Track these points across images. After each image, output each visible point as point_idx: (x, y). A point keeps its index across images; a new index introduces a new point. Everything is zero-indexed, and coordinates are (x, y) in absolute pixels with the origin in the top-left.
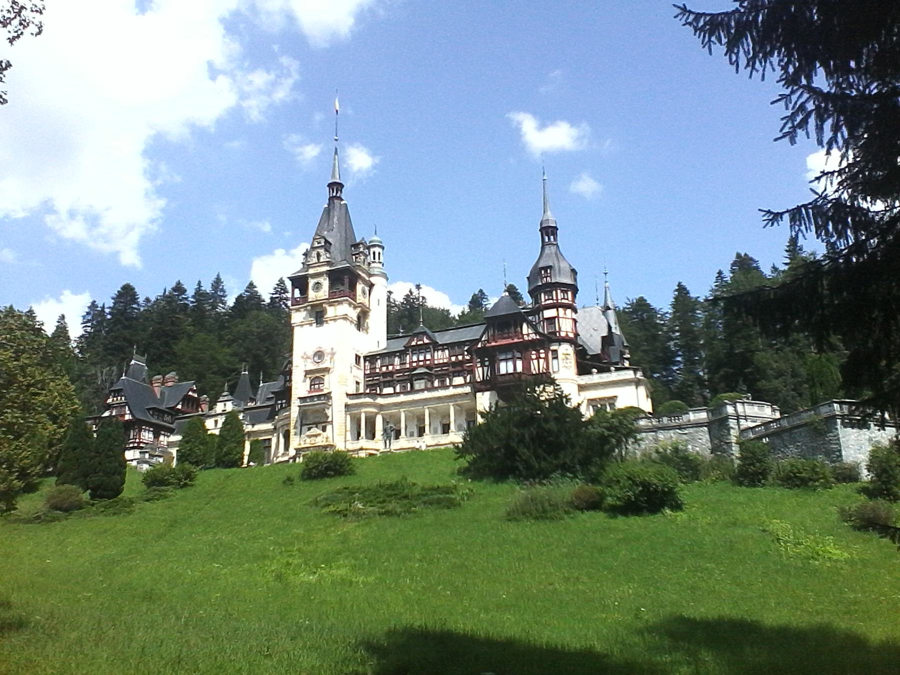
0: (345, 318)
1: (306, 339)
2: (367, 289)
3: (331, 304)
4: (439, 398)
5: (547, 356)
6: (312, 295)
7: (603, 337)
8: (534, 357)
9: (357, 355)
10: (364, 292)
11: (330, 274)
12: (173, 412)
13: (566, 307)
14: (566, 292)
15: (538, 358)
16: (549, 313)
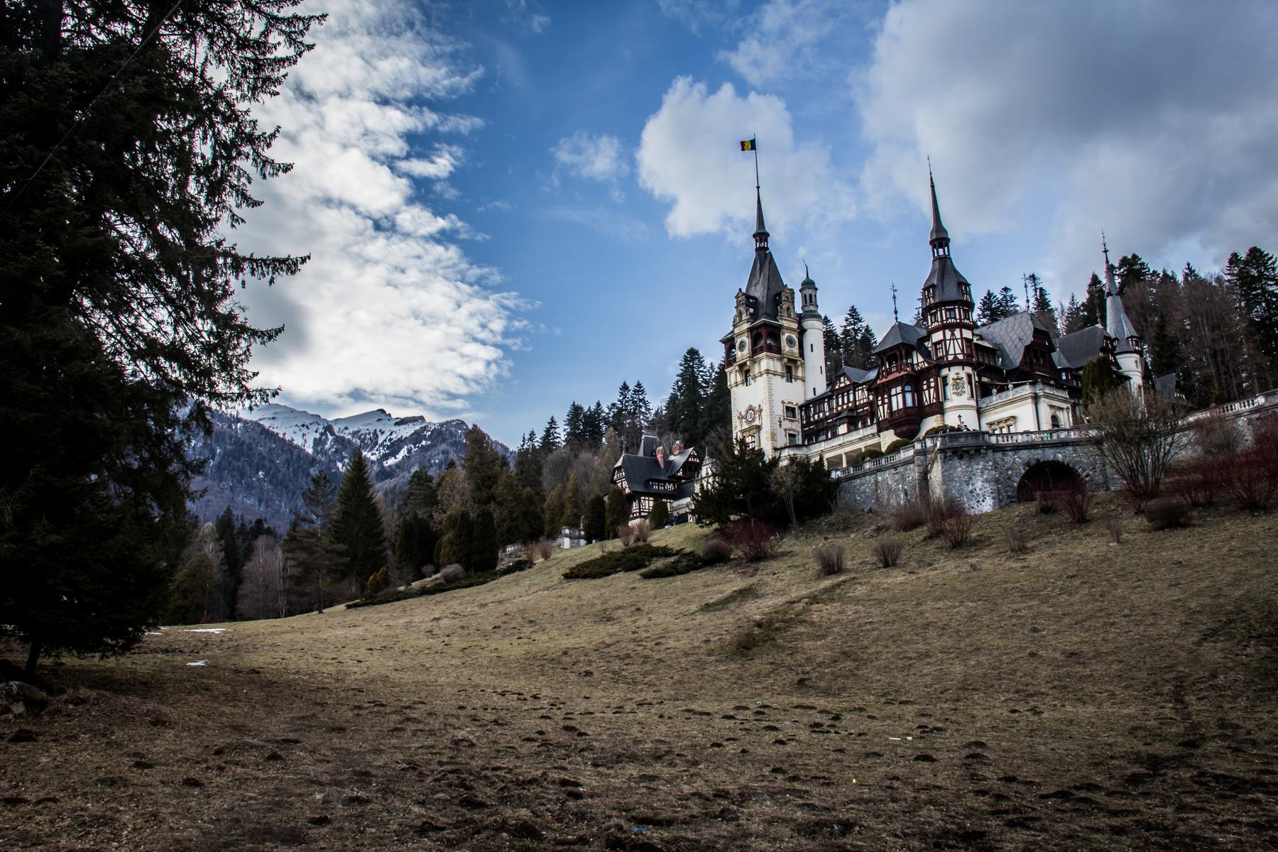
0: (768, 372)
1: (743, 397)
2: (795, 337)
3: (754, 362)
4: (851, 443)
5: (936, 382)
6: (738, 354)
7: (1027, 348)
9: (788, 409)
10: (790, 341)
11: (750, 330)
12: (674, 479)
13: (952, 327)
14: (953, 310)
15: (929, 388)
16: (937, 337)
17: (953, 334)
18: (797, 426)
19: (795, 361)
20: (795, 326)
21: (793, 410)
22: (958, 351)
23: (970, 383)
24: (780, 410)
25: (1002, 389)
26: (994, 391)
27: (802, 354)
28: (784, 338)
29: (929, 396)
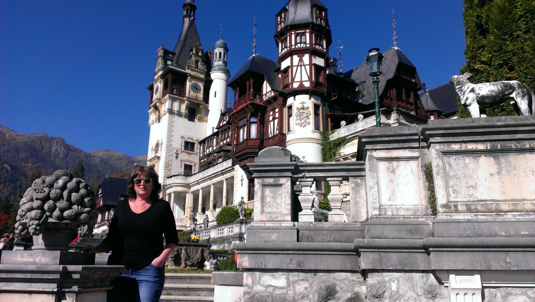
2: (201, 85)
8: (271, 118)
9: (187, 143)
10: (195, 88)
13: (301, 52)
14: (304, 34)
15: (274, 118)
17: (301, 60)
18: (194, 159)
19: (199, 105)
20: (202, 76)
21: (193, 144)
22: (305, 78)
23: (316, 114)
24: (178, 144)
25: (351, 120)
26: (343, 123)
27: (206, 98)
28: (188, 84)
29: (272, 128)
